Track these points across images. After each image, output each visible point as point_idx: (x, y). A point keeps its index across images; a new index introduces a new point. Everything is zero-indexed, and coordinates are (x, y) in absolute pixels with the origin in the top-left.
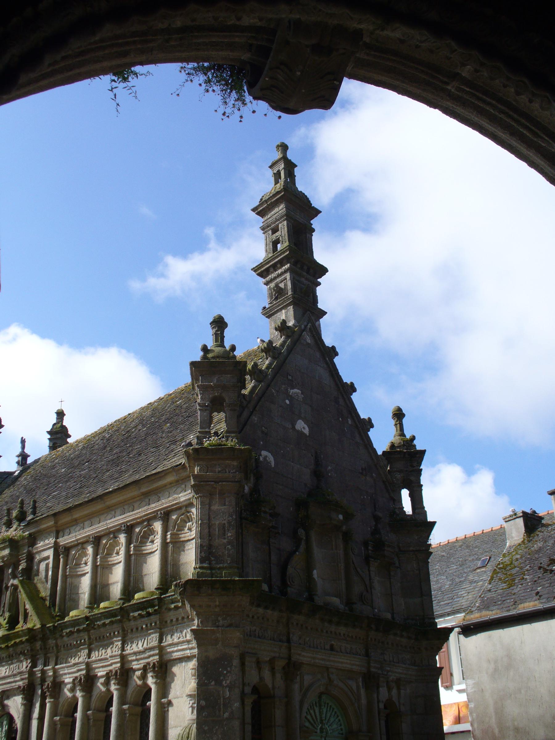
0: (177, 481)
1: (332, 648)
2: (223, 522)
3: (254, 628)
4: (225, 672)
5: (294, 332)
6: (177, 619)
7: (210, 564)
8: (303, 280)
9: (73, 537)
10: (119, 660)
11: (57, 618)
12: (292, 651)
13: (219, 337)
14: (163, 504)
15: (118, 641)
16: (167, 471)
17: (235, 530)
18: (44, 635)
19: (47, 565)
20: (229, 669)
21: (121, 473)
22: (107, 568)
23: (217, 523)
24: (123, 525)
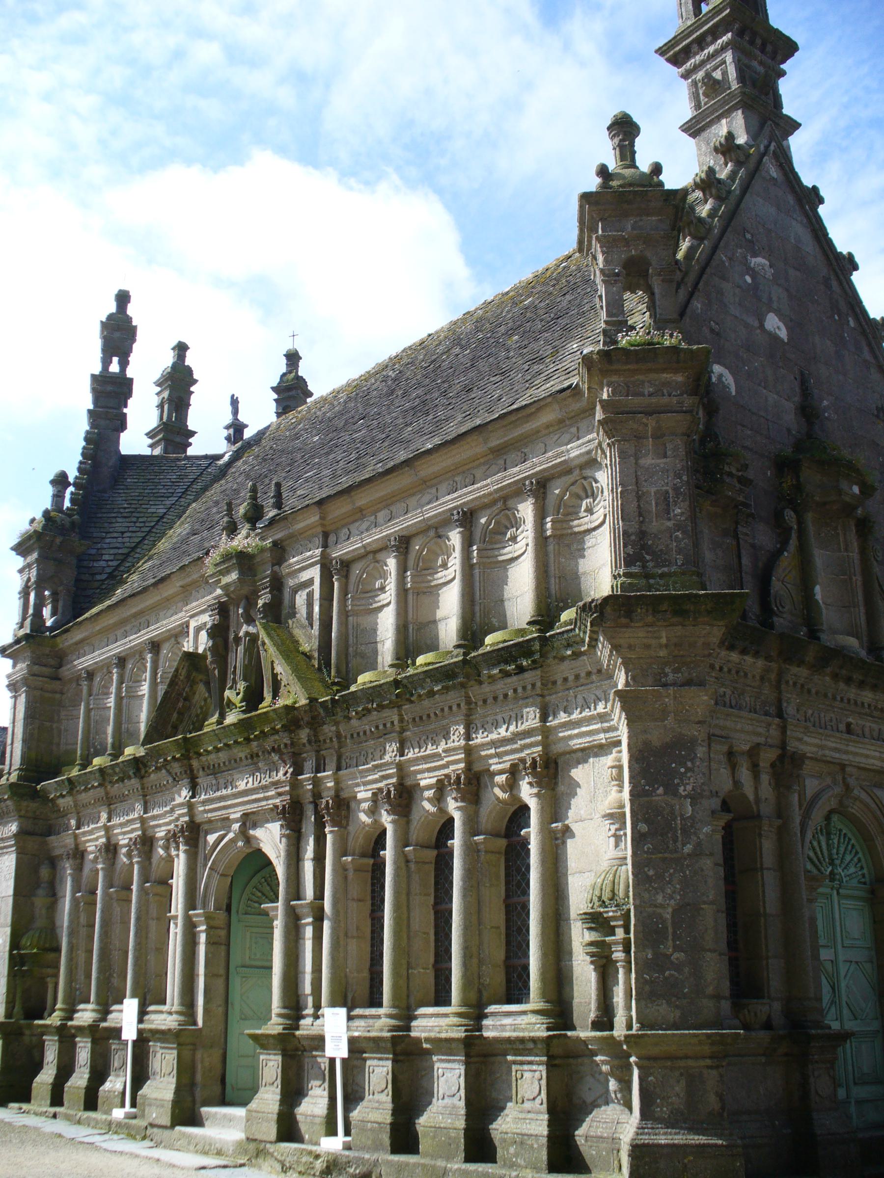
0: (561, 422)
1: (849, 730)
2: (665, 488)
3: (722, 689)
4: (683, 770)
5: (748, 156)
7: (644, 567)
8: (755, 64)
9: (356, 541)
11: (335, 688)
12: (788, 733)
13: (627, 152)
14: (534, 466)
16: (542, 403)
17: (687, 503)
18: (313, 718)
19: (310, 596)
20: (689, 764)
21: (438, 424)
23: (653, 490)
24: (455, 512)
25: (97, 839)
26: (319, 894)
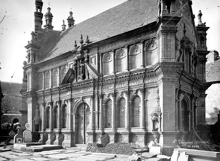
19: (95, 59)
26: (99, 110)
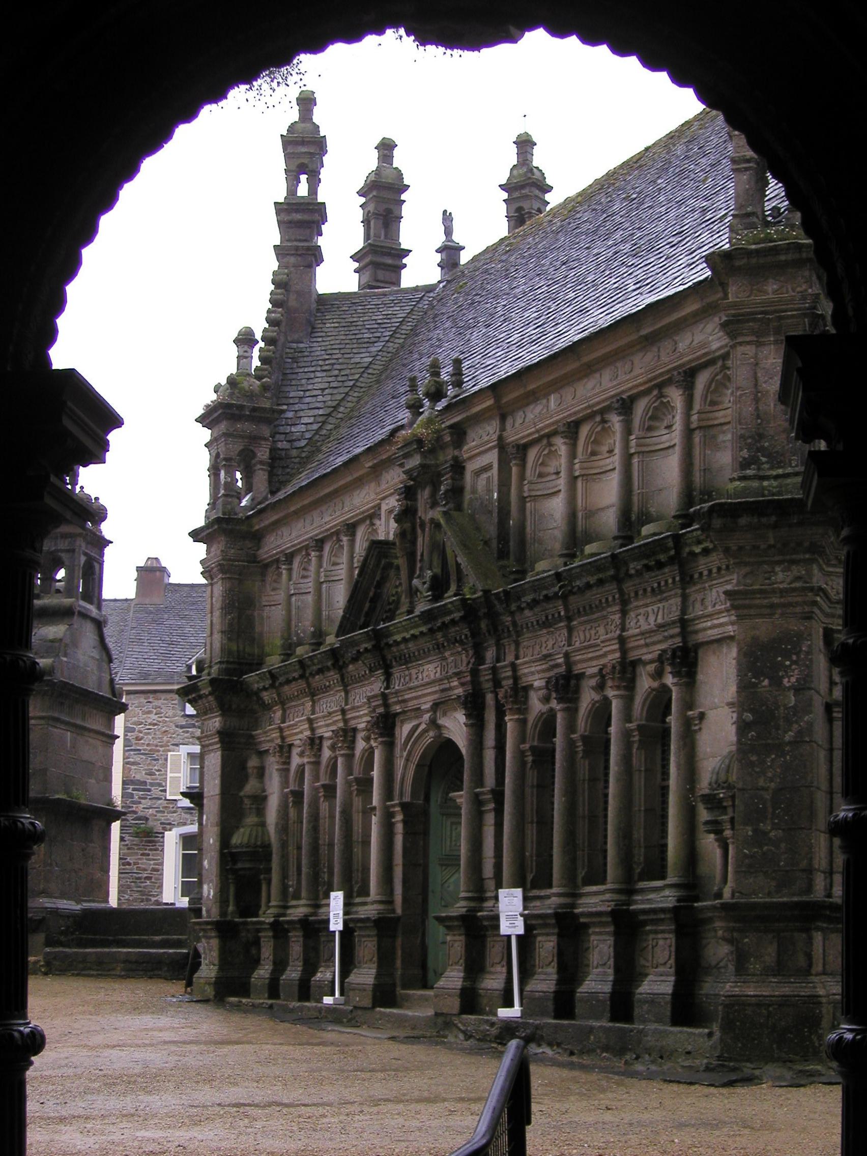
4: (788, 663)
6: (710, 571)
10: (617, 646)
11: (512, 577)
15: (614, 613)
20: (794, 657)
22: (594, 480)
25: (301, 732)
